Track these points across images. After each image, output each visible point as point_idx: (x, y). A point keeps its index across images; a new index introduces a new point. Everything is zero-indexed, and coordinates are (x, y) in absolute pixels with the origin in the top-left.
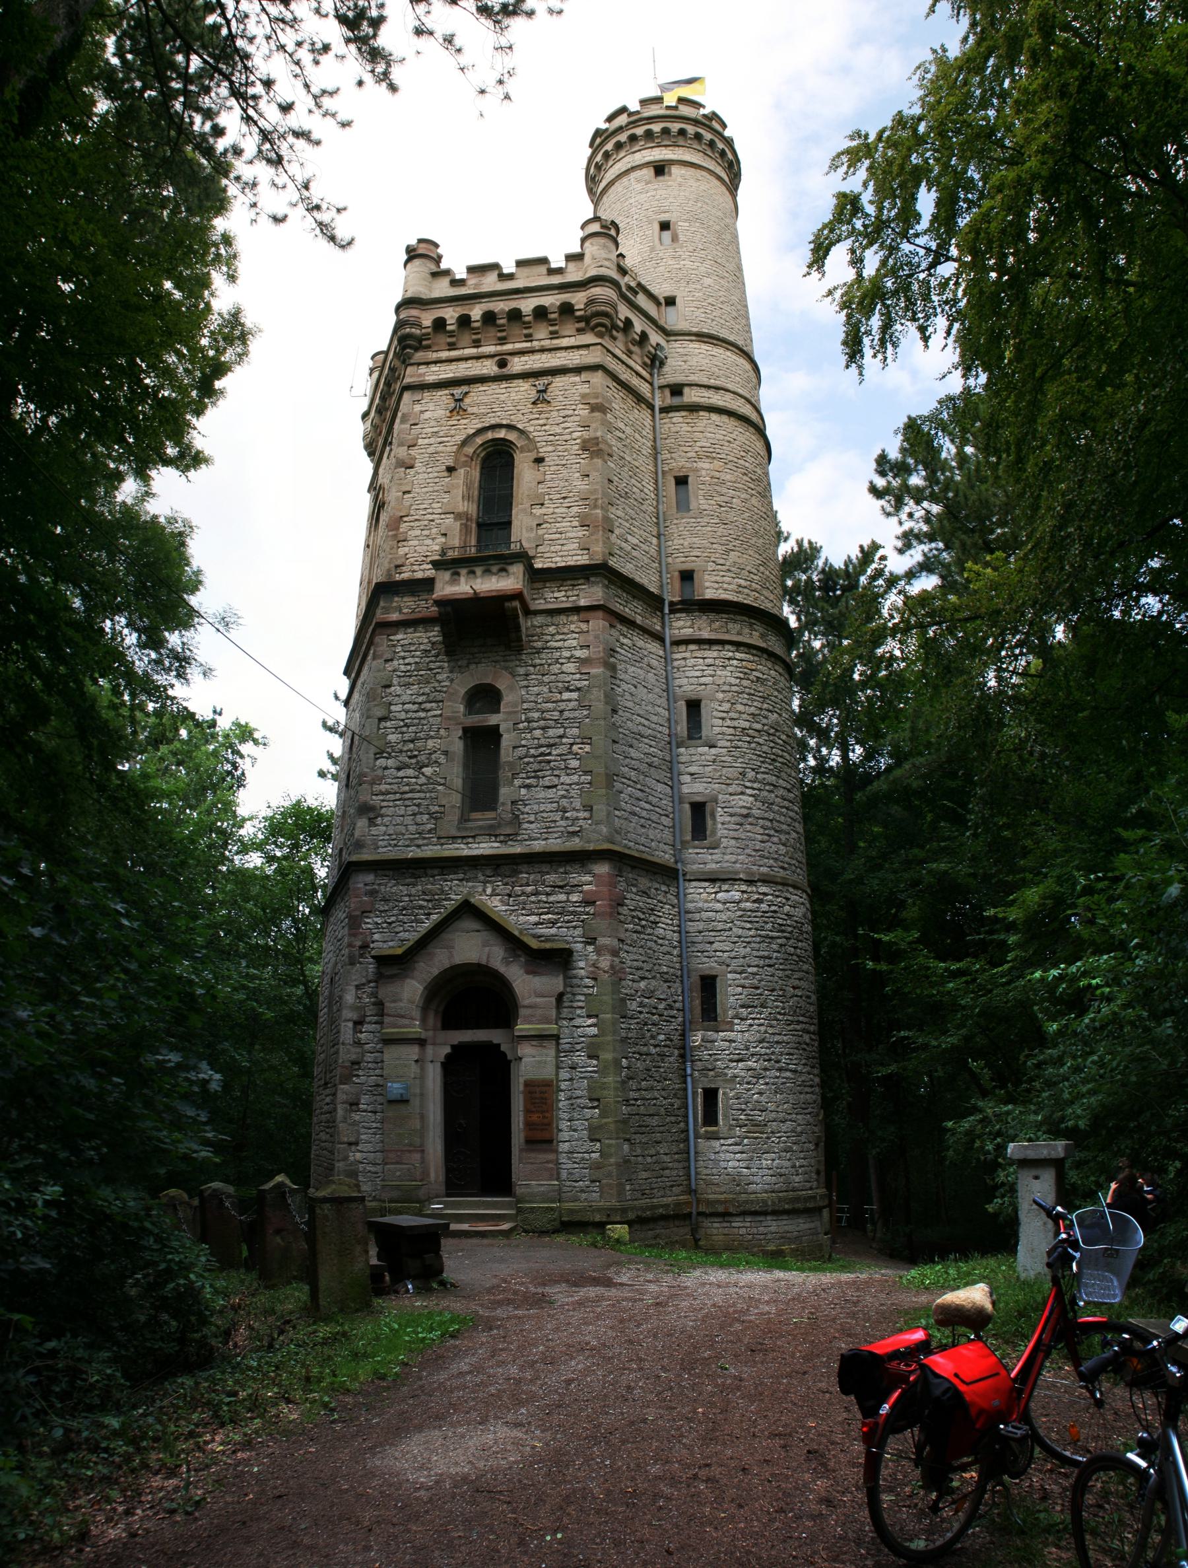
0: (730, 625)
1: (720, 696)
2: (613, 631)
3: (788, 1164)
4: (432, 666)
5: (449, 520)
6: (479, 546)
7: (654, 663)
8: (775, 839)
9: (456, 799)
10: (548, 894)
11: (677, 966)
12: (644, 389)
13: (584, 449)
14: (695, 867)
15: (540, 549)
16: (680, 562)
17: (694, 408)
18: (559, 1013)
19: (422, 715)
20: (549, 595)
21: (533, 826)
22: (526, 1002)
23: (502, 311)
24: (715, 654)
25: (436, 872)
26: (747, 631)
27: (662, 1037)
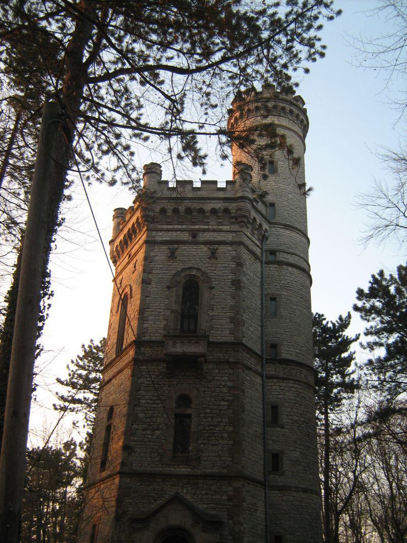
1: (287, 404)
5: (168, 313)
9: (171, 447)
10: (212, 495)
12: (258, 251)
14: (274, 484)
17: (281, 263)
19: (156, 406)
21: (206, 463)
23: (195, 208)
24: (285, 385)
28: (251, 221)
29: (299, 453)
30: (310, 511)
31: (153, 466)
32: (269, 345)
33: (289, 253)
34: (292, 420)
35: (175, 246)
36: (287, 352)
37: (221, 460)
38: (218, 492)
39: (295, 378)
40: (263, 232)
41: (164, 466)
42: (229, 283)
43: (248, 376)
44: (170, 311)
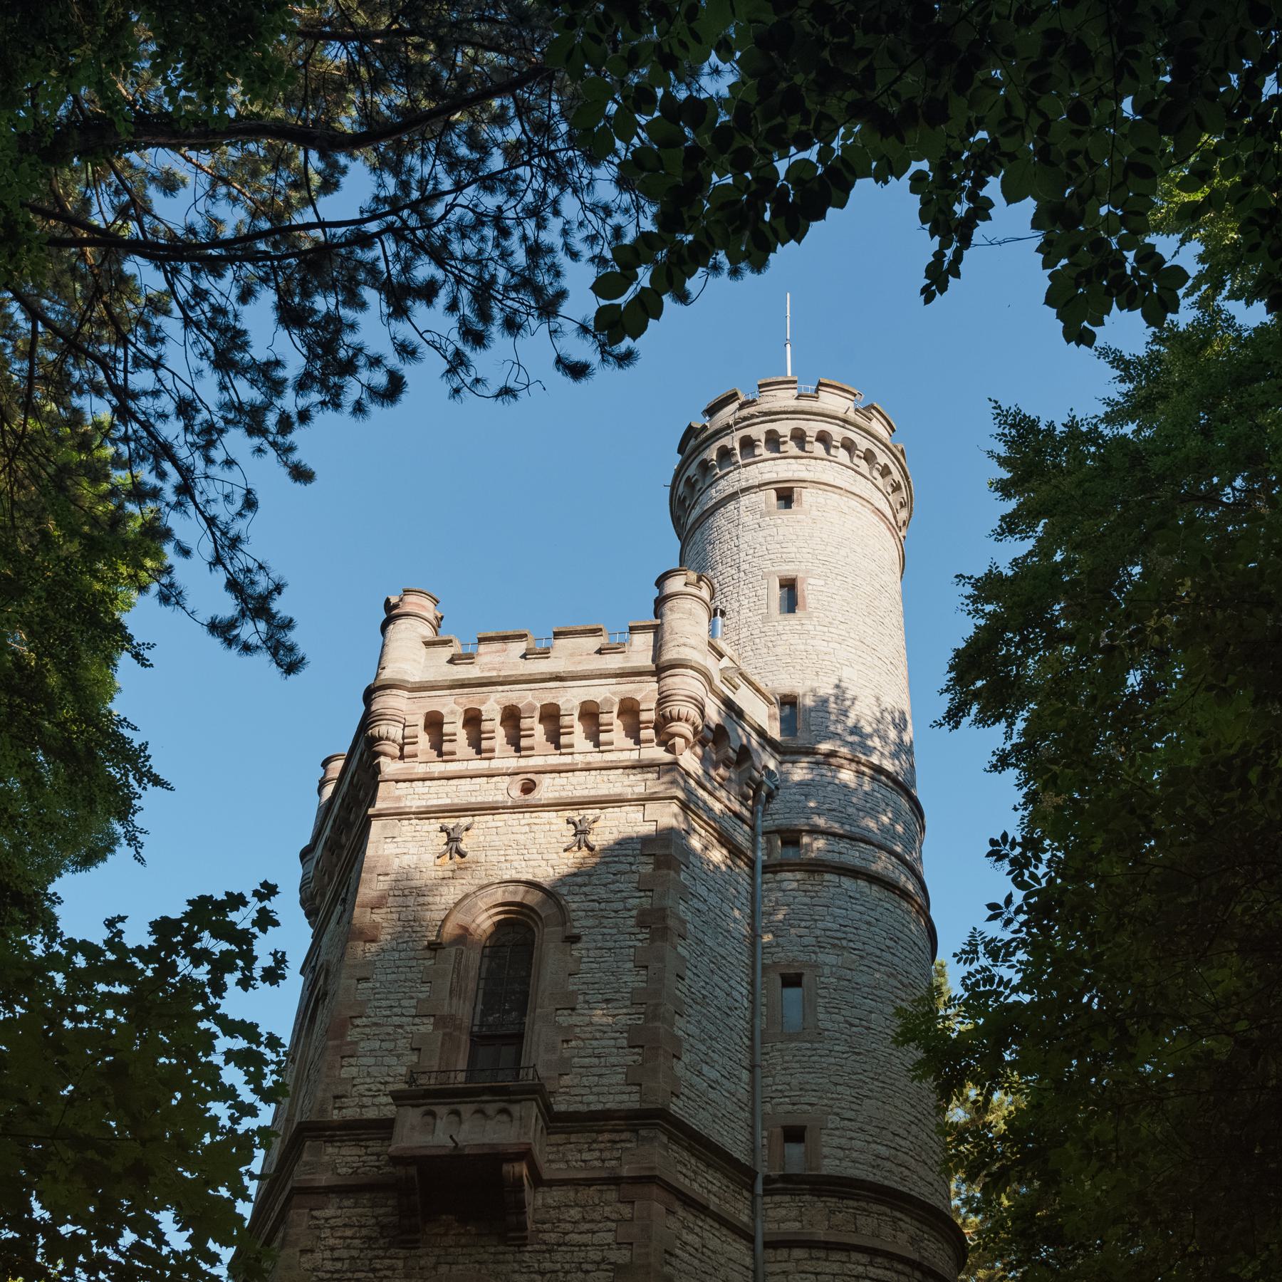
0: (862, 1220)
2: (673, 1223)
5: (427, 1027)
6: (471, 1070)
13: (641, 924)
15: (566, 1080)
17: (816, 867)
20: (573, 1156)
24: (835, 1268)
26: (887, 1230)
32: (778, 1131)
35: (465, 821)
36: (841, 1154)
39: (876, 1244)
42: (632, 922)
43: (691, 1231)
44: (432, 1019)
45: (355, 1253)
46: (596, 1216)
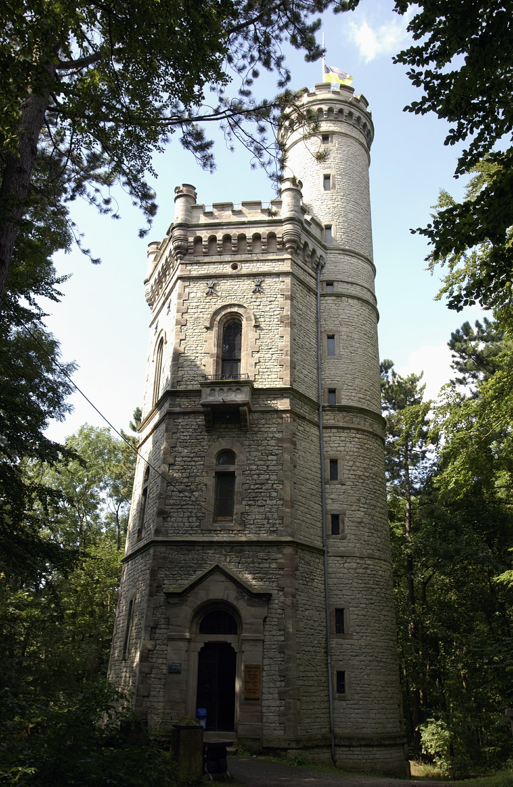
0: (354, 419)
1: (348, 457)
2: (295, 424)
3: (383, 717)
4: (198, 437)
7: (314, 439)
8: (375, 535)
9: (212, 509)
10: (259, 563)
11: (323, 603)
12: (312, 283)
16: (328, 384)
17: (339, 296)
18: (264, 628)
21: (252, 526)
22: (247, 622)
23: (235, 234)
24: (346, 435)
25: (200, 548)
26: (363, 422)
27: (316, 642)
28: (302, 246)
29: (363, 513)
30: (377, 579)
31: (192, 532)
32: (327, 390)
33: (348, 283)
34: (355, 475)
37: (270, 523)
38: (266, 560)
39: (359, 427)
40: (318, 260)
41: (204, 532)
43: (301, 426)
45: (190, 434)
46: (270, 422)
